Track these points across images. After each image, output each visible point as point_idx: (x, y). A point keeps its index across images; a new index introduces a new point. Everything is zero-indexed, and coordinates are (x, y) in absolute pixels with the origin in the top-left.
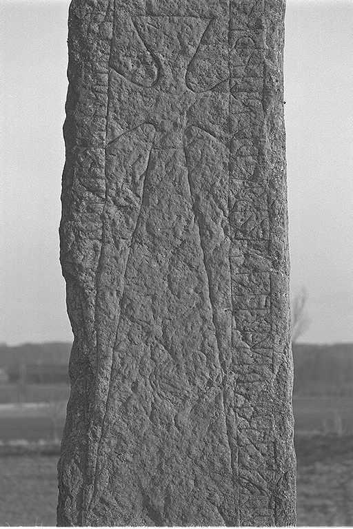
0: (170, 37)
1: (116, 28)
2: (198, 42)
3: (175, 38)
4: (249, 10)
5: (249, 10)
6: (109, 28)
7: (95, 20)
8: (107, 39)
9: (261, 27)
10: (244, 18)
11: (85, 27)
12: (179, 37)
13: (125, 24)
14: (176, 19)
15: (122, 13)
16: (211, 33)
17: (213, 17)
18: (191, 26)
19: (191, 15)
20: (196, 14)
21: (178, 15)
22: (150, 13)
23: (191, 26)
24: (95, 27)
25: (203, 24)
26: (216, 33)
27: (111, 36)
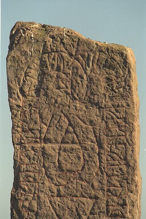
0: (70, 209)
1: (39, 204)
2: (88, 213)
3: (74, 210)
4: (118, 194)
5: (118, 194)
6: (35, 204)
7: (26, 199)
8: (33, 211)
9: (126, 205)
10: (115, 198)
11: (20, 204)
12: (77, 210)
13: (44, 202)
14: (75, 199)
15: (42, 195)
16: (96, 207)
17: (96, 198)
18: (84, 204)
19: (84, 197)
20: (86, 195)
21: (76, 196)
22: (59, 195)
23: (84, 204)
24: (27, 204)
25: (91, 202)
26: (99, 208)
27: (36, 209)
